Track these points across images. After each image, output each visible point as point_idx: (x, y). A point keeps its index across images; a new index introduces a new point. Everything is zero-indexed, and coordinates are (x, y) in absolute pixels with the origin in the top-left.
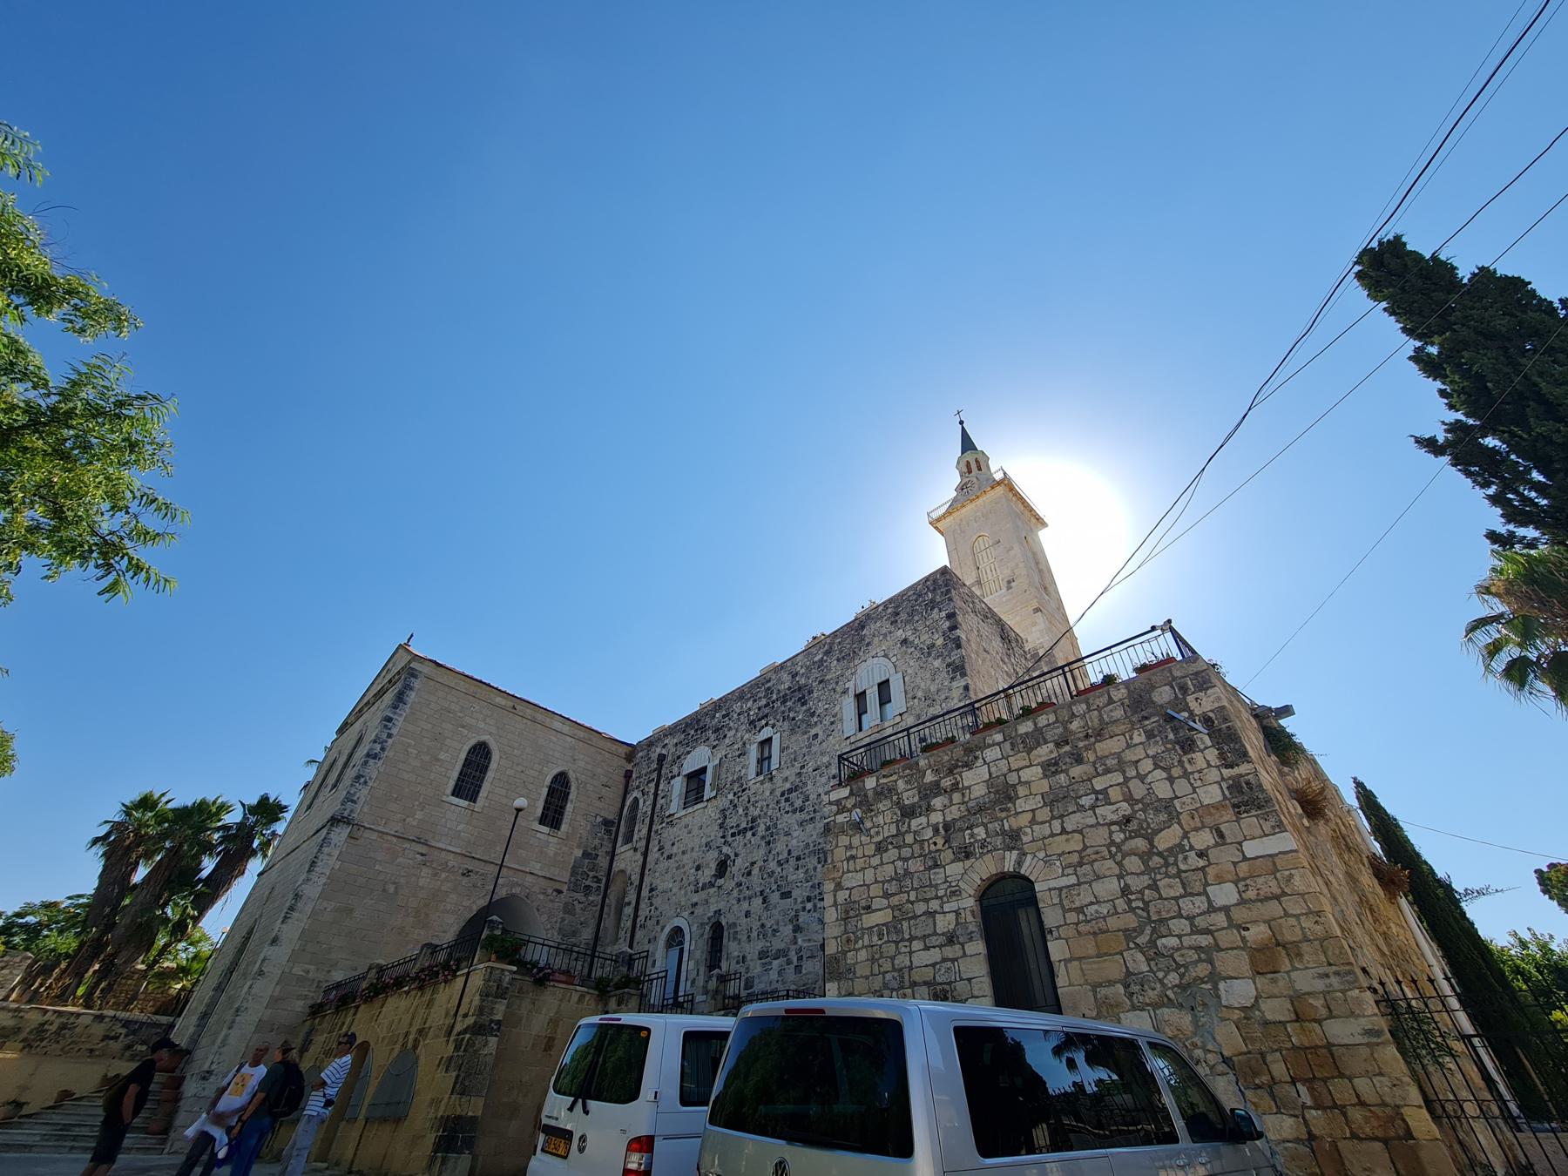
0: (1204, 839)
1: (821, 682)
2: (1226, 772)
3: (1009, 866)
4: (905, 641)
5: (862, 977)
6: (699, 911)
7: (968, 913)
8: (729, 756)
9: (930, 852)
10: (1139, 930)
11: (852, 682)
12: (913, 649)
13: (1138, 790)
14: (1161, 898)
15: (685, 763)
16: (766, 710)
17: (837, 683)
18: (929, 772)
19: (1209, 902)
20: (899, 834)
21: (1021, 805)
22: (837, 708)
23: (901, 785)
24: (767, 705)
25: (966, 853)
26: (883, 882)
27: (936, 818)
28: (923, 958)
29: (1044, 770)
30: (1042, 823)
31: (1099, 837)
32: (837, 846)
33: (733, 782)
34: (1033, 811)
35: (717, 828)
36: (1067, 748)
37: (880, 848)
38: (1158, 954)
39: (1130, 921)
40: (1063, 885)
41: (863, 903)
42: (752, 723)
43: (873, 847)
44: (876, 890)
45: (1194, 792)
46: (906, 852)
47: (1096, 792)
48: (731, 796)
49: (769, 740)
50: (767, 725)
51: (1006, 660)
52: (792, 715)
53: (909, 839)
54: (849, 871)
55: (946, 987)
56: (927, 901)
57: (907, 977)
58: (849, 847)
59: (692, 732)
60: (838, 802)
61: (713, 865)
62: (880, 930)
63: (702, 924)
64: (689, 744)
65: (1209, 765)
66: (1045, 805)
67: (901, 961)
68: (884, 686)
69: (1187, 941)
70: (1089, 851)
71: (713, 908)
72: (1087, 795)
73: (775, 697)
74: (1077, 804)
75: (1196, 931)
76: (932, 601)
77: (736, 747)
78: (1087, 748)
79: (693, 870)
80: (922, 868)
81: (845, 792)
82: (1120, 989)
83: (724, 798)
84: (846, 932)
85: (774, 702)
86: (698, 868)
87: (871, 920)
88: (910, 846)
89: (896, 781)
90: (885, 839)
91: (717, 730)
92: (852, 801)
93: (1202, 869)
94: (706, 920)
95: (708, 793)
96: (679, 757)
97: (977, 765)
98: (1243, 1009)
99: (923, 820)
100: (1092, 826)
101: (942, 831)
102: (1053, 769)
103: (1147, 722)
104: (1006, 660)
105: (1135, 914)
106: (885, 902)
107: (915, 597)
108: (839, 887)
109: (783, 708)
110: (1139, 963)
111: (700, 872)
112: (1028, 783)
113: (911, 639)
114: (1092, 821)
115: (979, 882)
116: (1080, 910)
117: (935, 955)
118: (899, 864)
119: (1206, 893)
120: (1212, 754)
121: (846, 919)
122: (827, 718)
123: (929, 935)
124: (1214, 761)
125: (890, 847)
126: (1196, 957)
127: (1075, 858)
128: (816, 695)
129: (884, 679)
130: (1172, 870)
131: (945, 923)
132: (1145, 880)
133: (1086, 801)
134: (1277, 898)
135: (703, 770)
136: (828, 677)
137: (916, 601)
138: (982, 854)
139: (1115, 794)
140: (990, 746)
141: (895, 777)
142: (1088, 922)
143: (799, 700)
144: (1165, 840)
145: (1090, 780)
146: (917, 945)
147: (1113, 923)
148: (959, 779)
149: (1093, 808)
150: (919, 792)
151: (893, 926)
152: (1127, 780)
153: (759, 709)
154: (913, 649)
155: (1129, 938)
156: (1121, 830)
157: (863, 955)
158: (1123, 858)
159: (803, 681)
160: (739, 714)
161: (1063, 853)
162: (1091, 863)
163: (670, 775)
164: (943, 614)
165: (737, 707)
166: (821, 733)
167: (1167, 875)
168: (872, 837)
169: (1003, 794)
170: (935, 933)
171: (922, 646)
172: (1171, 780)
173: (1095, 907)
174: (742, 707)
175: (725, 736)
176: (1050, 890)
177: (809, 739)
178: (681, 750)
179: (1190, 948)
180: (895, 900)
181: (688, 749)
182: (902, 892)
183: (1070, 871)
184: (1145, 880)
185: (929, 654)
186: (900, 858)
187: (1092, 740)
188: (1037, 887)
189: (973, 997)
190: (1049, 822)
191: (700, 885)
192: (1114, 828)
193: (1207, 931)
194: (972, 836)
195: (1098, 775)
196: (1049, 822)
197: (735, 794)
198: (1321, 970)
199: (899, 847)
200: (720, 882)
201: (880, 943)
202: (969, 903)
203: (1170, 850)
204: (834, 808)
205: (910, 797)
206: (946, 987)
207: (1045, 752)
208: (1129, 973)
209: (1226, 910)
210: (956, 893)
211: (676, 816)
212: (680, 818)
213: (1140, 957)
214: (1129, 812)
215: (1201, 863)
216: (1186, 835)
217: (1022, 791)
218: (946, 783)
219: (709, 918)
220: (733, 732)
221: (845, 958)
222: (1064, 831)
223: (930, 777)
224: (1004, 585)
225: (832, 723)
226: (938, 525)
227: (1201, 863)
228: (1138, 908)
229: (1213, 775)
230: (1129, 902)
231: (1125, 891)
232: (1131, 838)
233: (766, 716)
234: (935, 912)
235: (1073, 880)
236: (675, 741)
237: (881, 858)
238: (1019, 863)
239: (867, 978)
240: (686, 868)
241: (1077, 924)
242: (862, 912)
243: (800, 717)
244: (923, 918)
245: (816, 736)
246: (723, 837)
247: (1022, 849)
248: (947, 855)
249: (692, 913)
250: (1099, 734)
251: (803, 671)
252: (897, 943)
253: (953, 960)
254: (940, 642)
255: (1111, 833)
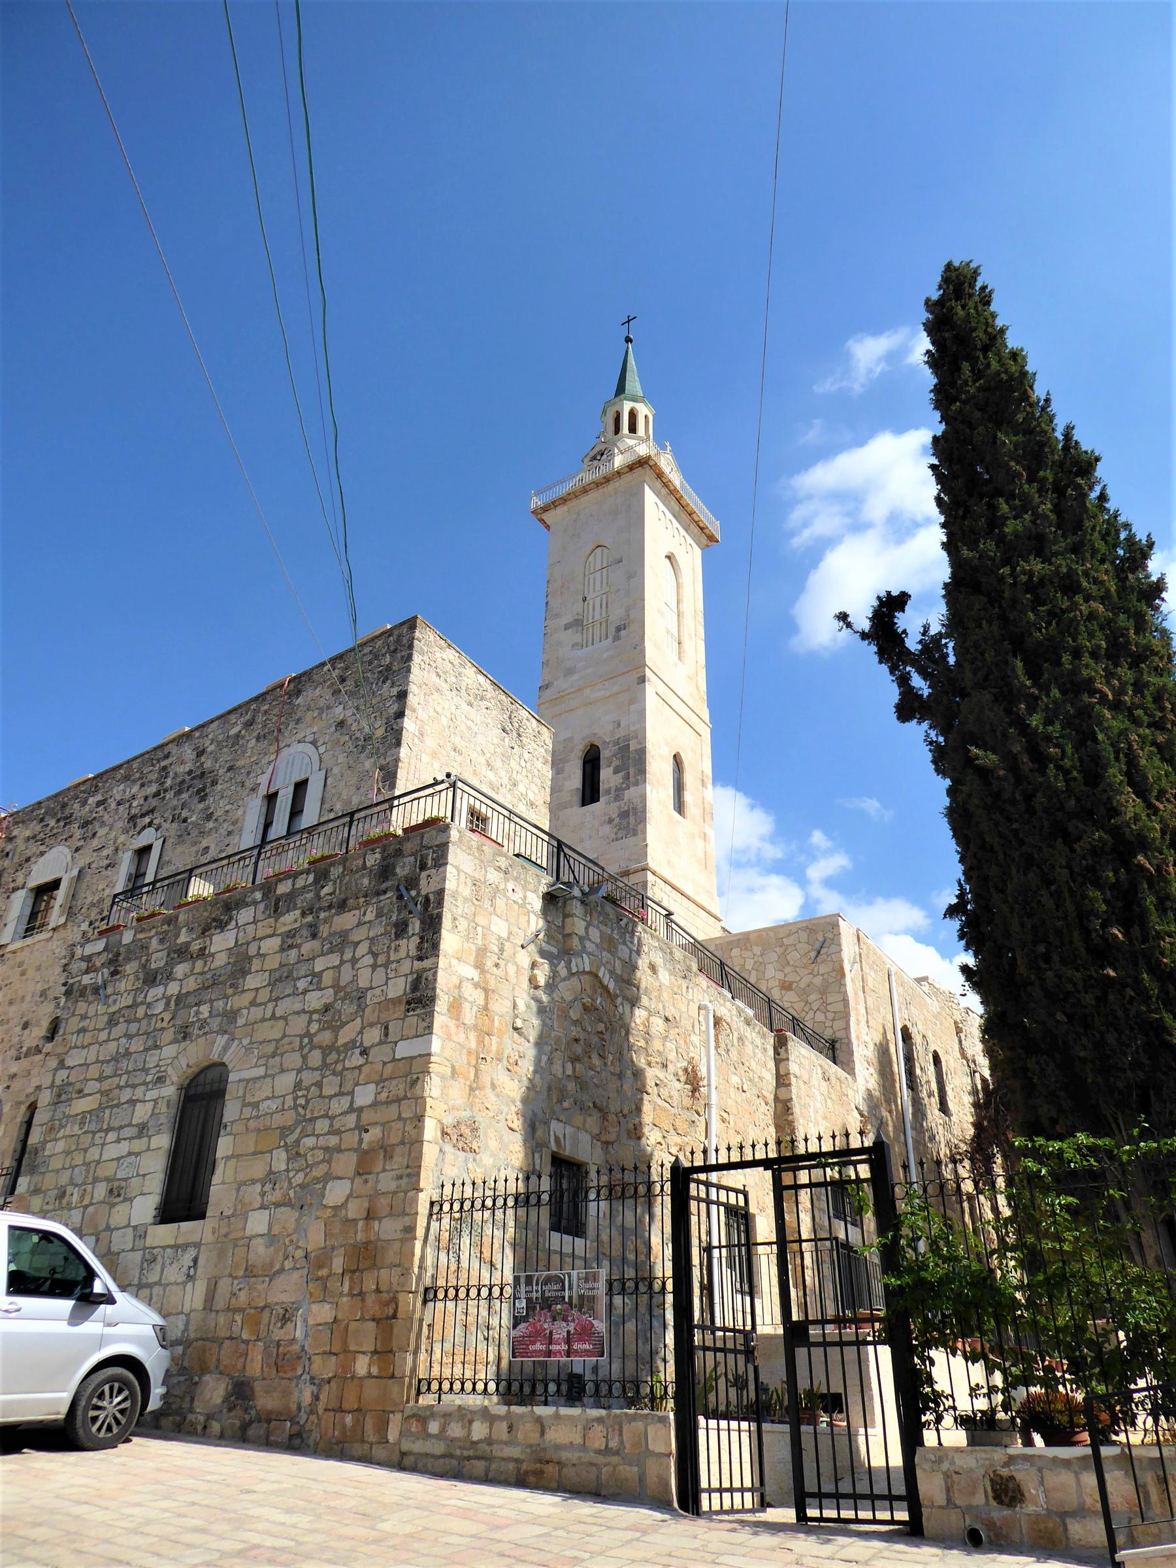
0: (372, 1036)
1: (230, 769)
2: (418, 965)
3: (214, 1057)
4: (341, 724)
5: (53, 1171)
6: (16, 1085)
7: (165, 1103)
8: (94, 866)
9: (155, 1030)
10: (290, 1129)
11: (266, 777)
12: (347, 738)
13: (346, 975)
14: (321, 1096)
15: (35, 868)
16: (154, 802)
17: (249, 773)
18: (184, 930)
19: (352, 1102)
20: (134, 1005)
21: (252, 982)
22: (240, 812)
23: (154, 943)
24: (156, 794)
25: (184, 1034)
26: (103, 1062)
27: (173, 989)
28: (112, 1151)
29: (283, 942)
30: (260, 1004)
31: (298, 1025)
32: (73, 1015)
33: (93, 905)
34: (257, 989)
35: (59, 970)
36: (309, 919)
37: (112, 1022)
38: (298, 1154)
39: (289, 1118)
40: (252, 1076)
41: (78, 1086)
42: (132, 819)
43: (106, 1018)
44: (94, 1071)
45: (386, 984)
46: (133, 1028)
47: (314, 975)
48: (85, 926)
49: (148, 849)
50: (150, 824)
51: (498, 764)
52: (185, 814)
53: (141, 1011)
54: (76, 1047)
55: (123, 1184)
56: (134, 1086)
57: (92, 1172)
58: (84, 1017)
59: (52, 823)
60: (88, 959)
61: (45, 1024)
62: (83, 1118)
63: (19, 1103)
64: (43, 841)
65: (408, 956)
66: (269, 985)
67: (93, 1153)
68: (301, 787)
69: (322, 1141)
70: (286, 1040)
71: (35, 1082)
72: (306, 976)
73: (169, 782)
74: (295, 985)
75: (332, 1132)
76: (389, 668)
77: (105, 852)
78: (325, 921)
79: (18, 1029)
80: (142, 1049)
81: (100, 945)
82: (258, 1187)
83: (75, 929)
84: (52, 1119)
85: (166, 791)
86: (25, 1026)
87: (82, 1105)
88: (139, 1021)
89: (151, 938)
90: (120, 1009)
91: (86, 824)
92: (104, 958)
93: (359, 1068)
94: (23, 1098)
95: (56, 917)
96: (28, 860)
97: (229, 927)
98: (335, 1208)
99: (160, 989)
100: (298, 1013)
101: (173, 1003)
102: (290, 941)
103: (382, 898)
104: (498, 764)
105: (296, 1111)
106: (98, 1085)
107: (370, 657)
108: (62, 1065)
109: (175, 802)
110: (280, 1160)
111: (27, 1032)
112: (264, 955)
113: (350, 721)
114: (298, 1007)
115: (185, 1067)
116: (256, 1105)
117: (124, 1147)
118: (123, 1041)
119: (352, 1093)
120: (415, 940)
121: (56, 1103)
122: (225, 825)
123: (126, 1126)
124: (413, 952)
125: (121, 1020)
126: (321, 1157)
127: (270, 1048)
128: (219, 787)
129: (303, 777)
130: (339, 1067)
131: (142, 1113)
132: (316, 1076)
133: (302, 984)
134: (398, 1100)
135: (55, 884)
136: (240, 763)
137: (370, 663)
138: (198, 1036)
139: (327, 978)
140: (247, 905)
141: (153, 932)
142: (257, 1117)
143: (198, 792)
144: (346, 1035)
145: (313, 959)
146: (112, 1136)
147: (278, 1120)
148: (208, 943)
149: (305, 992)
150: (168, 955)
151: (96, 1113)
152: (342, 962)
153: (146, 798)
154: (347, 738)
155: (283, 1137)
156: (319, 1021)
157: (60, 1146)
158: (310, 1051)
159: (208, 764)
160: (119, 804)
161: (264, 1041)
162: (282, 1055)
163: (12, 885)
164: (395, 691)
165: (118, 791)
166: (213, 846)
167: (334, 1073)
168: (109, 1006)
169: (241, 964)
170: (130, 1125)
171: (358, 735)
172: (374, 967)
173: (269, 1102)
174: (124, 791)
175: (94, 834)
176: (240, 1081)
177: (197, 852)
178: (34, 848)
179: (321, 1148)
180: (106, 1085)
181: (42, 848)
182: (115, 1075)
183: (262, 1062)
184: (316, 1076)
185: (364, 747)
186: (126, 1035)
187: (333, 911)
188: (232, 1077)
189: (142, 1194)
190: (265, 1004)
191: (24, 1049)
192: (315, 1017)
193: (338, 1132)
194: (197, 1013)
195: (322, 954)
196: (265, 1004)
197: (91, 924)
198: (399, 1172)
199: (128, 1022)
200: (48, 1047)
201: (80, 1132)
202: (169, 1091)
203: (345, 1045)
204: (84, 965)
205: (158, 961)
206: (123, 1184)
207: (290, 919)
208: (271, 1172)
209: (360, 1110)
210: (160, 1080)
211: (10, 948)
212: (14, 952)
213: (284, 1156)
214: (330, 1000)
215: (361, 1061)
216: (361, 1032)
217: (256, 965)
218: (195, 947)
219: (27, 1096)
220: (105, 830)
221: (44, 1149)
222: (273, 1017)
223: (183, 938)
224: (612, 630)
225: (230, 833)
226: (545, 517)
227: (361, 1061)
228: (300, 1105)
229: (406, 967)
230: (295, 1099)
231: (298, 1085)
232: (324, 1029)
233: (152, 811)
234: (138, 1101)
235: (261, 1071)
236: (28, 833)
237: (109, 1034)
238: (225, 1049)
239: (57, 1171)
240: (11, 1023)
241: (248, 1119)
242: (74, 1096)
243: (194, 819)
244: (125, 1106)
245: (207, 848)
246: (65, 984)
247: (232, 1034)
248: (169, 1035)
249: (8, 1087)
250: (342, 906)
251: (211, 748)
252: (94, 1133)
253: (137, 1154)
254: (380, 732)
255: (310, 1021)
